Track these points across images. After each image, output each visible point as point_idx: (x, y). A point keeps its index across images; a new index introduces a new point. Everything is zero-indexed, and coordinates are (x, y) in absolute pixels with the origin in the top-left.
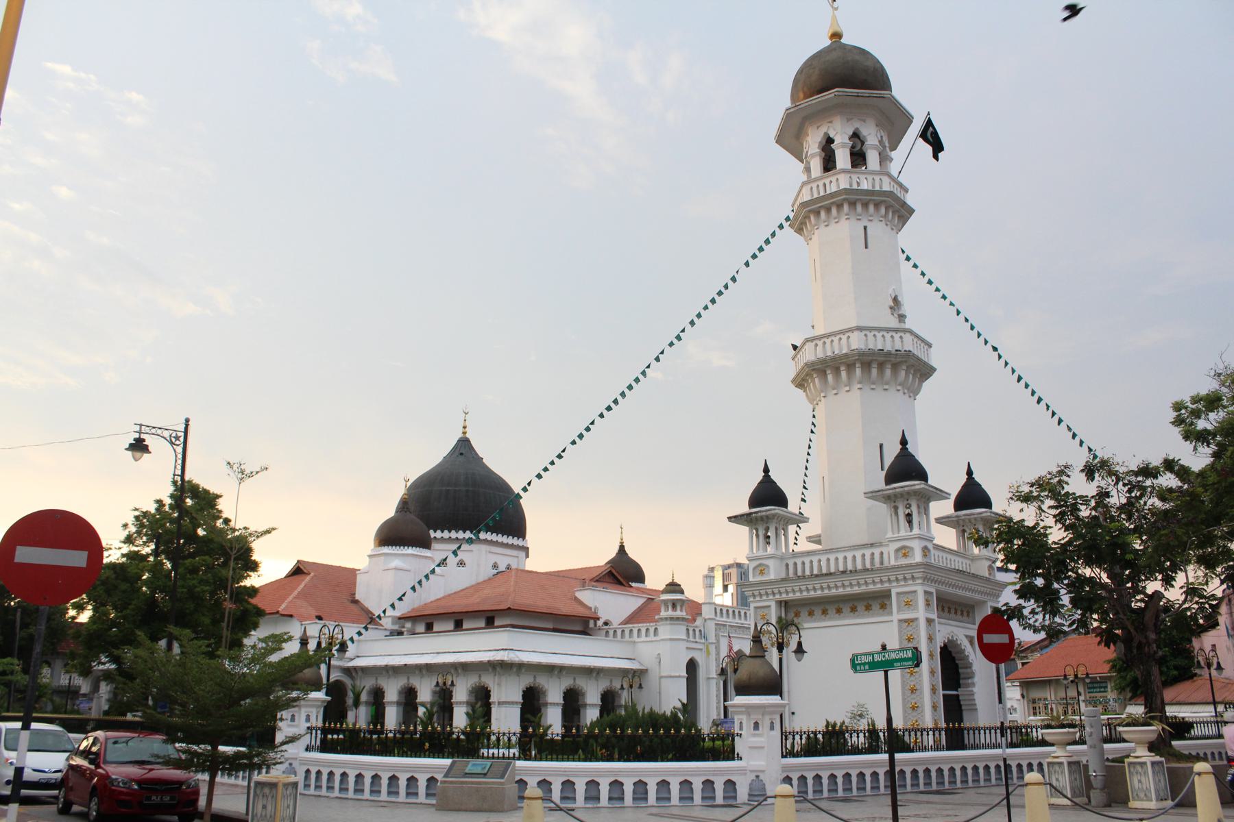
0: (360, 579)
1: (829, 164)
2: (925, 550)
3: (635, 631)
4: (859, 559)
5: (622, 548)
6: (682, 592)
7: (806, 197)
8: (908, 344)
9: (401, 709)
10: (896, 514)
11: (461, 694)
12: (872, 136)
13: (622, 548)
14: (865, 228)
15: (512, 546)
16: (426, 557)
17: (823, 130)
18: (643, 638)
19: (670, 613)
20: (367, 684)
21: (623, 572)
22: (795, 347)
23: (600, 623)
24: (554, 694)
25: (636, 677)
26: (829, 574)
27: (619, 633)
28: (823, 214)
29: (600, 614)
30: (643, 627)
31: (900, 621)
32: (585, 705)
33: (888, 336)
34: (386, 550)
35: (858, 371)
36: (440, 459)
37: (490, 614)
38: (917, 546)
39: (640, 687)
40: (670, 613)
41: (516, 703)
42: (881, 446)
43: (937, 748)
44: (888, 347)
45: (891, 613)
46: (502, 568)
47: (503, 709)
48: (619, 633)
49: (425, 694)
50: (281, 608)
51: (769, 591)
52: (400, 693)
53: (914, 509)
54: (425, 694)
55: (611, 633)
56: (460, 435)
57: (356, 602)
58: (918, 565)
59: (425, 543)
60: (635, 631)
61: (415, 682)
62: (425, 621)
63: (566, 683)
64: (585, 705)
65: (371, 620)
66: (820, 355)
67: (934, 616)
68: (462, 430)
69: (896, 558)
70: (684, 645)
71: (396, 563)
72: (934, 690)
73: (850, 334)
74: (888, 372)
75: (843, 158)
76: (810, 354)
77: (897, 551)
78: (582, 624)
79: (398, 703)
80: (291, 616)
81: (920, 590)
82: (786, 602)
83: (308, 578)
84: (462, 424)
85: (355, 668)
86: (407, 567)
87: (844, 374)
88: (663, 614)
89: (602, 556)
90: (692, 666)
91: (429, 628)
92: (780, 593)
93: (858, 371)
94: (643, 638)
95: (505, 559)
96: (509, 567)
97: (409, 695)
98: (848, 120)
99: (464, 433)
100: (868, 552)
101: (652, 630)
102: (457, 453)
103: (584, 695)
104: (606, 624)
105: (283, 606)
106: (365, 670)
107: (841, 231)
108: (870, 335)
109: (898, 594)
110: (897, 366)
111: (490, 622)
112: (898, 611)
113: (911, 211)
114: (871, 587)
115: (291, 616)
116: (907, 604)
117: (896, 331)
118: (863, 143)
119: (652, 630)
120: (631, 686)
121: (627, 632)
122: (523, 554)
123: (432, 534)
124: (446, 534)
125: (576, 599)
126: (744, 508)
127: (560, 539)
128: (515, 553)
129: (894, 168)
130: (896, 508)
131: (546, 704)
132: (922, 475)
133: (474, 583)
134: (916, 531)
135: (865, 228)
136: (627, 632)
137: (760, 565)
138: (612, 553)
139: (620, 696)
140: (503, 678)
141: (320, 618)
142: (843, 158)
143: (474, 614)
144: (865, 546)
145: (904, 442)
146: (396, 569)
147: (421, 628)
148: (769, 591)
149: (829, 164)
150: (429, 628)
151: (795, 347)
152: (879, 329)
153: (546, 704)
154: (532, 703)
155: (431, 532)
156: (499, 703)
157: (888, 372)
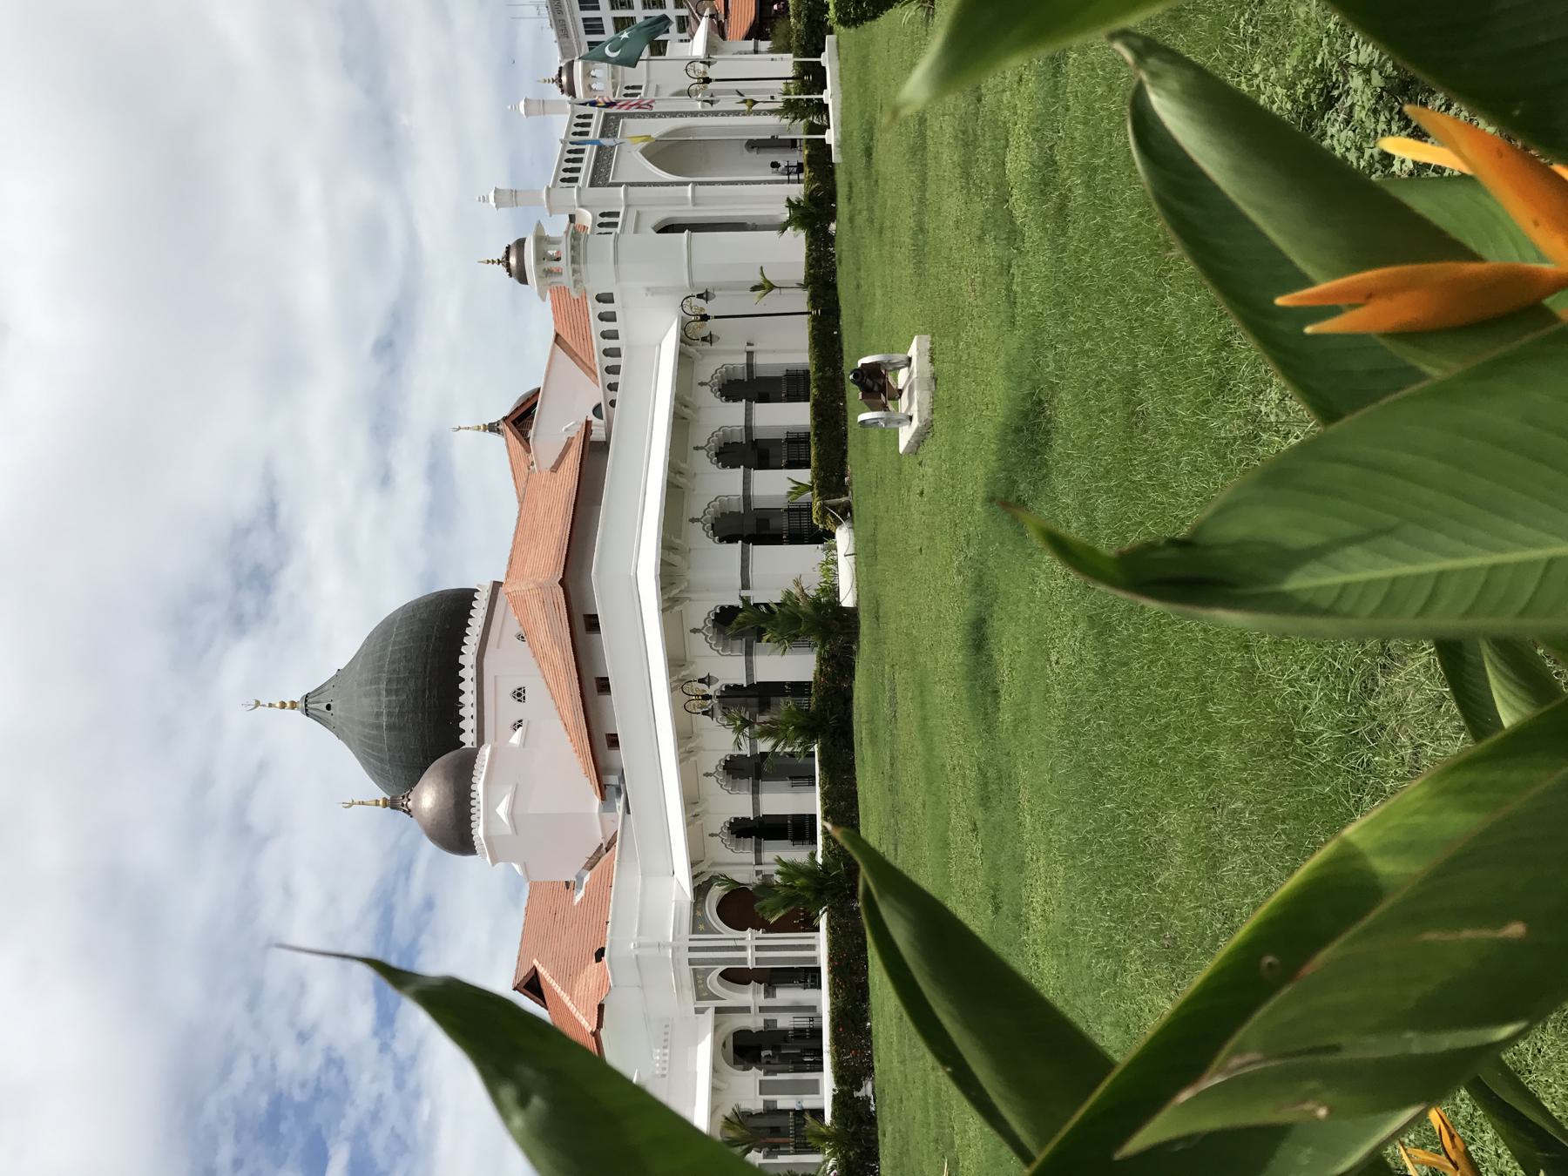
6: (520, 243)
9: (763, 784)
11: (729, 669)
34: (479, 833)
37: (580, 624)
40: (564, 265)
55: (612, 395)
56: (298, 714)
62: (602, 745)
63: (704, 464)
68: (287, 711)
70: (629, 239)
80: (601, 1007)
83: (541, 970)
84: (277, 711)
85: (695, 877)
88: (566, 279)
89: (499, 447)
90: (668, 228)
95: (507, 622)
99: (293, 705)
105: (584, 1023)
111: (592, 623)
115: (601, 1007)
150: (613, 741)
156: (745, 585)
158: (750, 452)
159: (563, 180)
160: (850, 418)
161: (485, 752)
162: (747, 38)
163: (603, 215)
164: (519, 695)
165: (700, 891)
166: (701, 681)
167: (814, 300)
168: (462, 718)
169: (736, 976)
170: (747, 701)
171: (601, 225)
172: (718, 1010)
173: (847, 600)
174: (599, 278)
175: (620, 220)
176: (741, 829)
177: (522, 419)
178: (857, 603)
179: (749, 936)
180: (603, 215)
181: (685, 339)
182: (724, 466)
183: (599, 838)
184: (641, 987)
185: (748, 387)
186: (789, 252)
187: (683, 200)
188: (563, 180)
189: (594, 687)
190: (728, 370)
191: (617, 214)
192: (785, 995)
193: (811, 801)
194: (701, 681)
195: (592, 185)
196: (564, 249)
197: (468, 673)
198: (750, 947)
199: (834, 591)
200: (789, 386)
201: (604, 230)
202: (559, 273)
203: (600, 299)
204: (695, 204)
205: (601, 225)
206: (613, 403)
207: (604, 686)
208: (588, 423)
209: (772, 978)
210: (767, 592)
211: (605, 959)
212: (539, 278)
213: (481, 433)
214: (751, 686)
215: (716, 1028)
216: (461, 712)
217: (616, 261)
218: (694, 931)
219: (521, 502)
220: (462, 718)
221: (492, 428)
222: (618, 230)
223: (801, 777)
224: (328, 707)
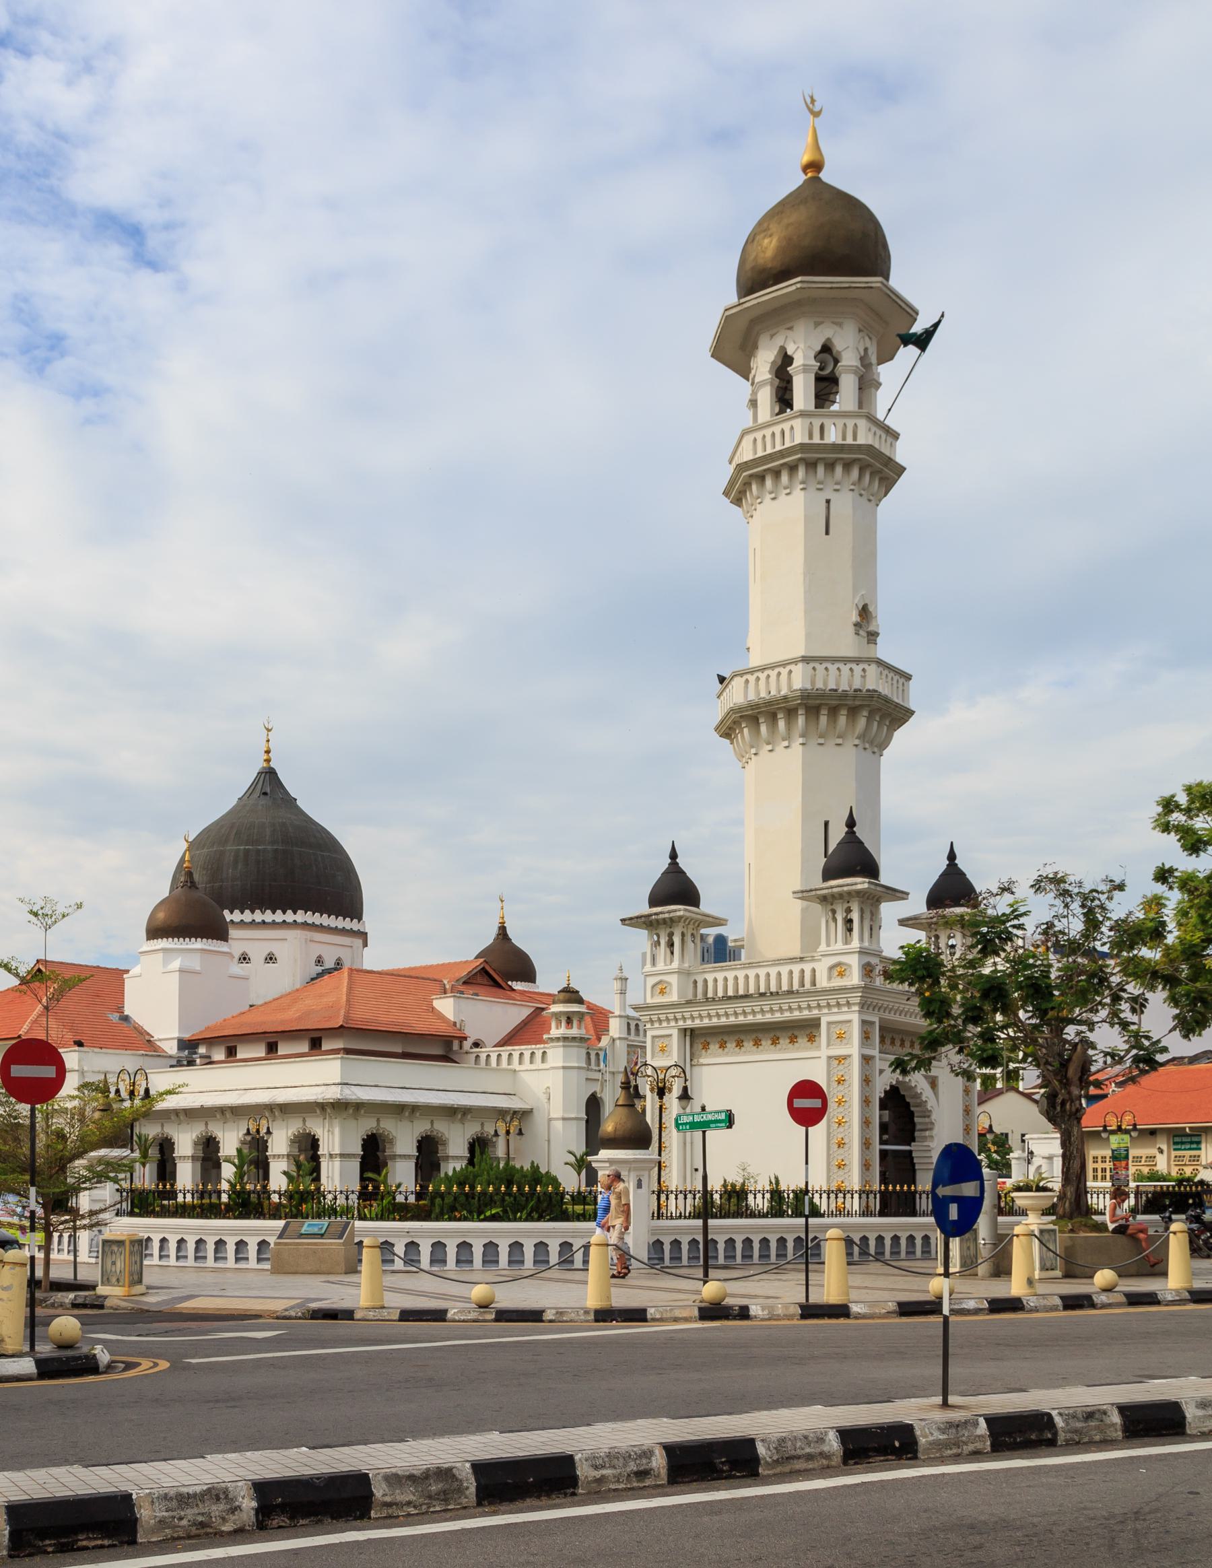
0: (129, 985)
1: (784, 399)
2: (867, 970)
3: (516, 1056)
4: (786, 976)
5: (503, 930)
7: (746, 455)
8: (873, 681)
9: (199, 1164)
10: (835, 920)
11: (280, 1143)
12: (849, 346)
13: (503, 930)
14: (828, 501)
17: (779, 341)
18: (527, 1065)
21: (504, 967)
22: (722, 679)
23: (467, 1045)
24: (404, 1141)
25: (518, 1119)
26: (746, 996)
28: (769, 482)
29: (467, 1032)
30: (527, 1050)
31: (830, 1058)
33: (845, 669)
35: (801, 720)
36: (234, 802)
38: (854, 962)
39: (520, 1133)
41: (354, 1155)
42: (826, 824)
43: (866, 1212)
44: (844, 686)
45: (818, 1048)
46: (329, 963)
51: (671, 1016)
52: (196, 1144)
53: (855, 916)
57: (126, 1019)
58: (853, 989)
59: (218, 932)
60: (516, 1056)
63: (421, 1127)
66: (752, 696)
67: (875, 1052)
69: (830, 978)
70: (584, 1074)
72: (866, 1144)
73: (792, 667)
74: (842, 720)
75: (803, 391)
76: (737, 695)
77: (831, 968)
79: (194, 1158)
81: (855, 1018)
82: (692, 1030)
87: (781, 724)
88: (555, 1032)
91: (231, 1052)
92: (684, 1019)
93: (801, 720)
94: (527, 1065)
95: (331, 949)
96: (339, 965)
97: (208, 1151)
98: (817, 324)
100: (796, 969)
101: (539, 1054)
107: (788, 509)
108: (820, 668)
109: (829, 1023)
110: (857, 710)
112: (828, 1045)
113: (901, 470)
114: (797, 1013)
116: (840, 1037)
117: (858, 661)
118: (836, 361)
119: (539, 1054)
121: (505, 1056)
122: (358, 942)
123: (228, 915)
124: (247, 916)
126: (645, 909)
127: (413, 923)
128: (346, 940)
129: (882, 401)
130: (834, 912)
132: (869, 868)
134: (855, 944)
135: (828, 501)
136: (505, 1056)
137: (660, 982)
138: (488, 937)
139: (494, 1145)
140: (336, 1122)
141: (80, 1044)
142: (803, 391)
143: (292, 1035)
144: (792, 960)
145: (851, 823)
147: (219, 1054)
148: (671, 1016)
149: (784, 399)
151: (722, 679)
152: (834, 660)
154: (373, 1155)
155: (226, 913)
156: (331, 1156)
157: (842, 720)
164: (271, 958)
168: (253, 912)
171: (597, 1054)
174: (556, 1055)
182: (418, 1141)
195: (629, 1046)
197: (290, 916)
201: (593, 1057)
203: (544, 1053)
205: (597, 1054)
211: (77, 1048)
214: (267, 1158)
216: (258, 911)
217: (564, 1068)
220: (253, 912)
224: (265, 794)
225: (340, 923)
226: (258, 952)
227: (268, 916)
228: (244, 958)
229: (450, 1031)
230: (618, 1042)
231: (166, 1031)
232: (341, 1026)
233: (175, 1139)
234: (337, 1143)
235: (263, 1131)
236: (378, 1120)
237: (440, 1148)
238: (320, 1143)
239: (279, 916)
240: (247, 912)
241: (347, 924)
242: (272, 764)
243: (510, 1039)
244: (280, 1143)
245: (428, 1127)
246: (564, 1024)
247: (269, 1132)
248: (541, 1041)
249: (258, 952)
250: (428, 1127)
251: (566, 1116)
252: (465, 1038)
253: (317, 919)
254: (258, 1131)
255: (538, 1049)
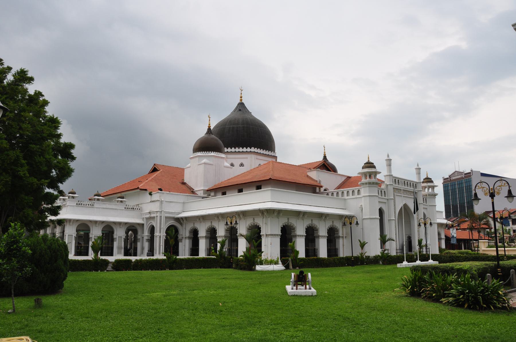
0: (186, 171)
3: (345, 193)
5: (325, 157)
9: (208, 240)
11: (242, 229)
15: (268, 156)
16: (222, 157)
18: (351, 196)
19: (368, 180)
20: (189, 227)
23: (322, 190)
25: (348, 220)
27: (335, 194)
29: (322, 184)
30: (350, 189)
32: (318, 237)
34: (199, 154)
37: (259, 184)
41: (277, 235)
47: (269, 239)
48: (335, 194)
49: (221, 232)
50: (141, 186)
52: (207, 231)
54: (221, 232)
55: (330, 194)
56: (239, 101)
60: (345, 193)
61: (215, 224)
62: (222, 190)
63: (307, 222)
64: (318, 237)
65: (193, 192)
68: (240, 99)
70: (377, 200)
71: (205, 160)
78: (313, 188)
79: (206, 237)
83: (159, 172)
84: (240, 96)
85: (182, 218)
86: (212, 163)
88: (364, 180)
90: (381, 212)
94: (351, 196)
97: (212, 233)
101: (356, 192)
102: (237, 110)
103: (317, 230)
104: (325, 190)
106: (187, 219)
111: (259, 188)
119: (356, 192)
120: (351, 223)
121: (340, 193)
125: (308, 176)
131: (295, 236)
133: (249, 170)
136: (340, 193)
140: (269, 219)
141: (160, 190)
146: (205, 163)
150: (224, 194)
153: (295, 236)
154: (286, 236)
155: (225, 148)
156: (266, 235)
158: (311, 236)
159: (395, 180)
160: (310, 269)
161: (223, 155)
162: (446, 236)
163: (385, 192)
164: (242, 165)
165: (178, 220)
166: (236, 221)
167: (357, 258)
168: (235, 148)
169: (152, 229)
170: (232, 235)
171: (381, 191)
172: (143, 224)
173: (258, 268)
174: (365, 191)
175: (383, 197)
176: (195, 233)
177: (326, 166)
178: (257, 271)
179: (163, 234)
180: (385, 192)
181: (347, 217)
182: (306, 229)
183: (196, 189)
184: (151, 202)
185: (332, 236)
186: (374, 249)
187: (391, 215)
188: (395, 180)
189: (240, 188)
190: (338, 231)
191: (385, 196)
192: (146, 245)
193: (202, 254)
194: (236, 221)
196: (373, 180)
197: (249, 149)
198: (160, 235)
199: (261, 263)
200: (332, 249)
202: (366, 179)
203: (359, 191)
204: (389, 220)
205: (381, 191)
206: (328, 194)
207: (240, 191)
208: (322, 187)
209: (151, 241)
210: (265, 242)
212: (364, 173)
213: (323, 154)
214: (237, 237)
215: (138, 224)
217: (369, 196)
218: (166, 218)
219: (298, 166)
220: (235, 148)
221: (325, 157)
222: (380, 196)
223: (209, 252)
224: (240, 110)
225: (267, 152)
226: (237, 163)
227: (241, 150)
228: (232, 165)
229: (315, 184)
230: (389, 186)
231: (199, 187)
232: (270, 179)
233: (199, 229)
234: (270, 231)
235: (234, 223)
236: (288, 219)
237: (315, 232)
238: (262, 229)
239: (245, 150)
240: (233, 148)
241: (270, 153)
242: (243, 101)
243: (339, 187)
244: (242, 229)
245: (310, 222)
246: (368, 177)
247: (236, 223)
248: (358, 186)
249: (237, 163)
250: (310, 222)
251: (371, 217)
252: (322, 187)
253: (259, 151)
254: (231, 223)
255: (356, 189)
